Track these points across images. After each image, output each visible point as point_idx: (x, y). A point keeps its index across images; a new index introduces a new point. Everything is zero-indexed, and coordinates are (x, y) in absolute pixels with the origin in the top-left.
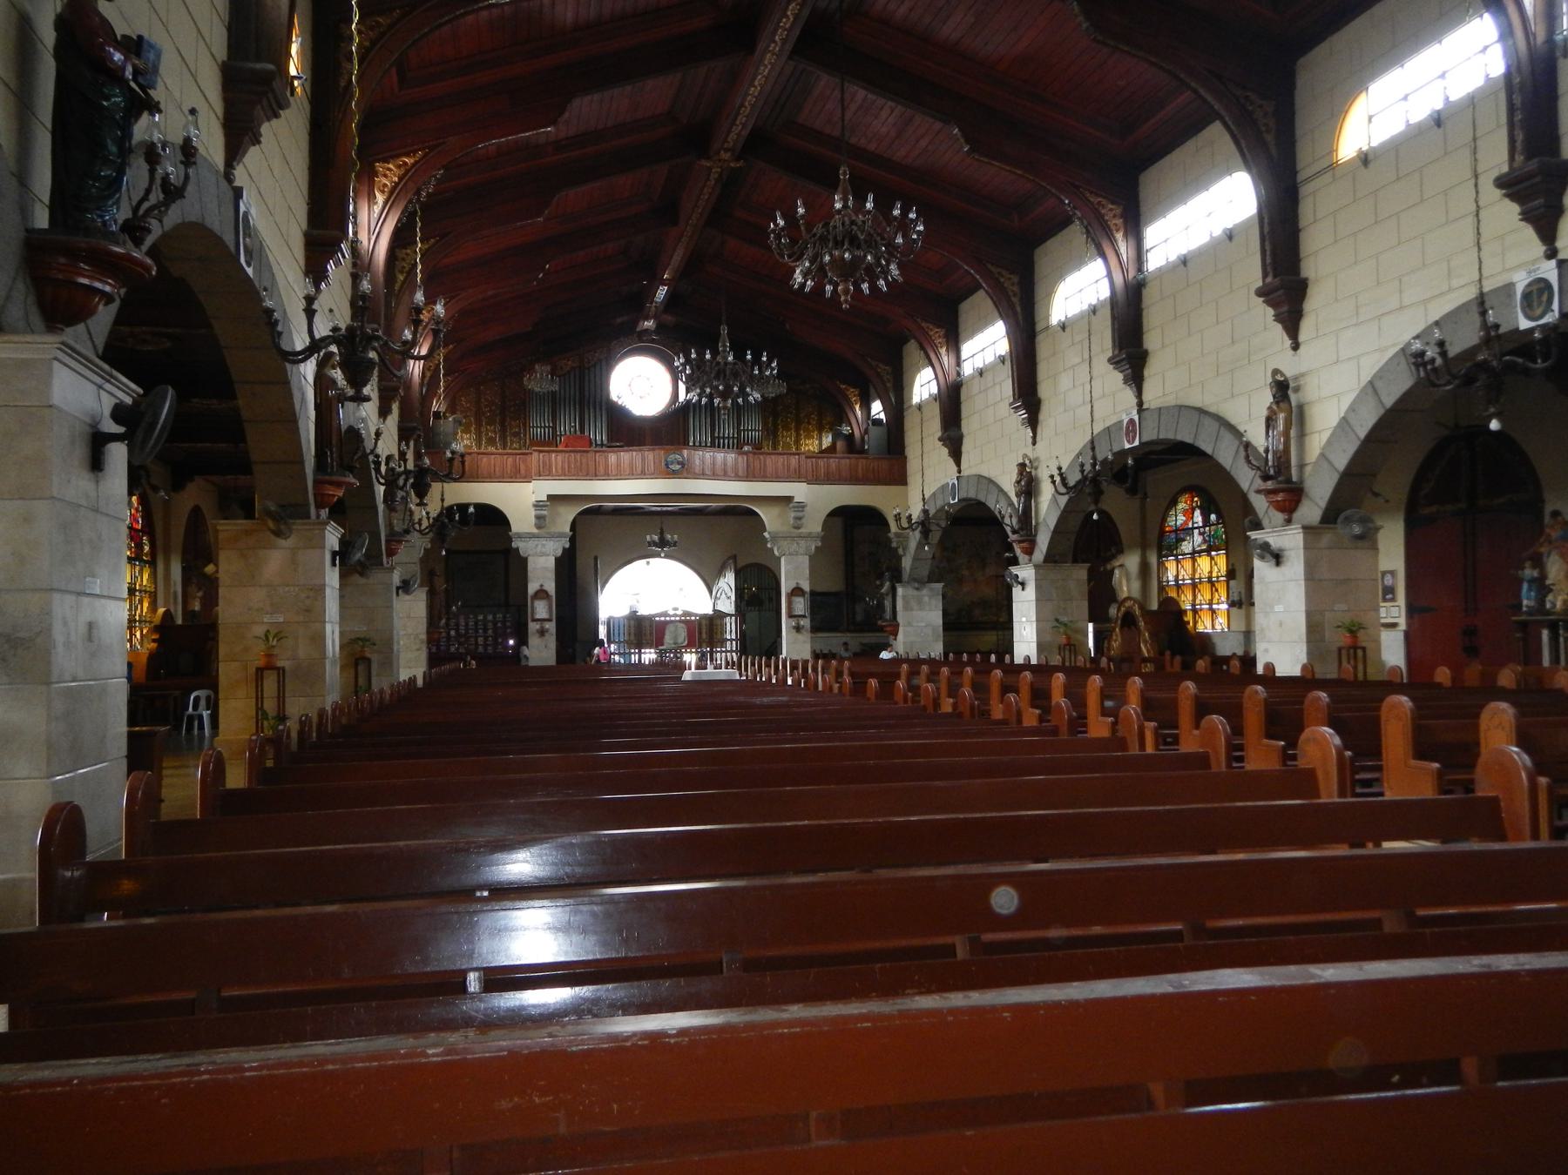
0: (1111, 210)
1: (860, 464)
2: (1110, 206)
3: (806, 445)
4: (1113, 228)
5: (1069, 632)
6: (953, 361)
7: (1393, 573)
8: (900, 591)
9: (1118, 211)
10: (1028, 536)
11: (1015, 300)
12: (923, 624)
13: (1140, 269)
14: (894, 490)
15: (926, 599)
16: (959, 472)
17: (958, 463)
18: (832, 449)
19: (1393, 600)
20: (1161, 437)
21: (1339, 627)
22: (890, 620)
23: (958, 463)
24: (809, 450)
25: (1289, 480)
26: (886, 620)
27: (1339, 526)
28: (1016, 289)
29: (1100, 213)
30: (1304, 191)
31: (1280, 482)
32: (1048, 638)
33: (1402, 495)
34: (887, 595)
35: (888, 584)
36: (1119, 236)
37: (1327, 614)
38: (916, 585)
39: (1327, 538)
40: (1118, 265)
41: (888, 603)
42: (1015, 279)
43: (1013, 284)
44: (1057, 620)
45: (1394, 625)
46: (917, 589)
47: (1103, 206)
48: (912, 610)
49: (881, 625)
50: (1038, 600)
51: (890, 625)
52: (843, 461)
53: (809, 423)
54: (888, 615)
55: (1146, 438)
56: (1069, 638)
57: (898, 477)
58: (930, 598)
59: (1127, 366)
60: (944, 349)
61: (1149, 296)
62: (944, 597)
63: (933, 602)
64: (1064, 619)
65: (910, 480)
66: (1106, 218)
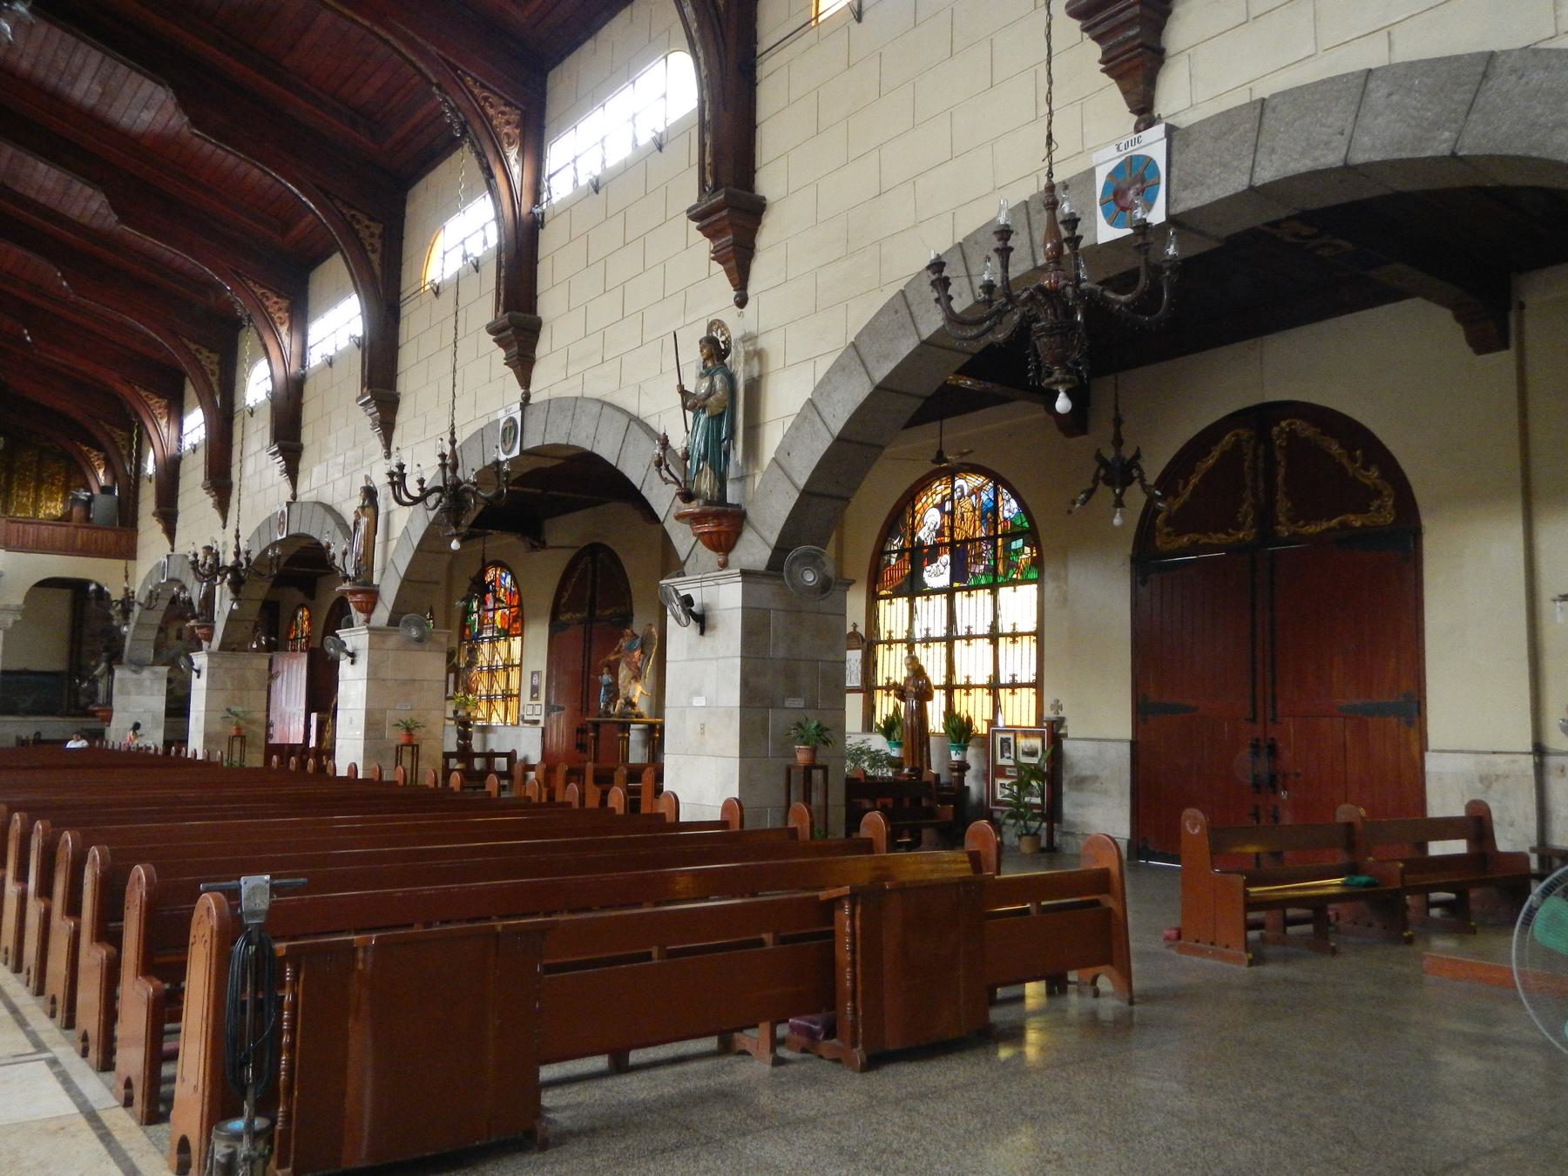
0: (276, 303)
1: (80, 533)
2: (275, 299)
3: (47, 507)
4: (277, 321)
5: (242, 723)
6: (173, 433)
7: (538, 673)
8: (118, 673)
9: (284, 304)
10: (205, 621)
11: (214, 379)
12: (142, 710)
13: (303, 366)
14: (121, 563)
15: (148, 683)
16: (173, 550)
17: (172, 541)
18: (66, 518)
19: (537, 698)
20: (301, 531)
21: (398, 725)
22: (104, 705)
23: (172, 541)
24: (51, 514)
25: (369, 582)
26: (99, 705)
27: (400, 628)
28: (215, 368)
29: (263, 304)
30: (405, 311)
31: (358, 584)
32: (218, 728)
33: (547, 603)
34: (102, 676)
35: (103, 665)
36: (283, 330)
37: (389, 714)
38: (133, 667)
39: (393, 641)
40: (280, 358)
41: (101, 687)
42: (215, 357)
43: (211, 363)
44: (229, 710)
45: (536, 722)
46: (135, 672)
47: (268, 298)
48: (128, 693)
49: (92, 711)
50: (208, 689)
51: (103, 711)
52: (58, 529)
53: (53, 484)
54: (101, 699)
55: (291, 532)
56: (239, 729)
57: (128, 551)
58: (152, 680)
59: (281, 458)
60: (165, 420)
61: (309, 391)
62: (169, 681)
63: (156, 686)
64: (238, 709)
65: (139, 554)
66: (270, 310)
